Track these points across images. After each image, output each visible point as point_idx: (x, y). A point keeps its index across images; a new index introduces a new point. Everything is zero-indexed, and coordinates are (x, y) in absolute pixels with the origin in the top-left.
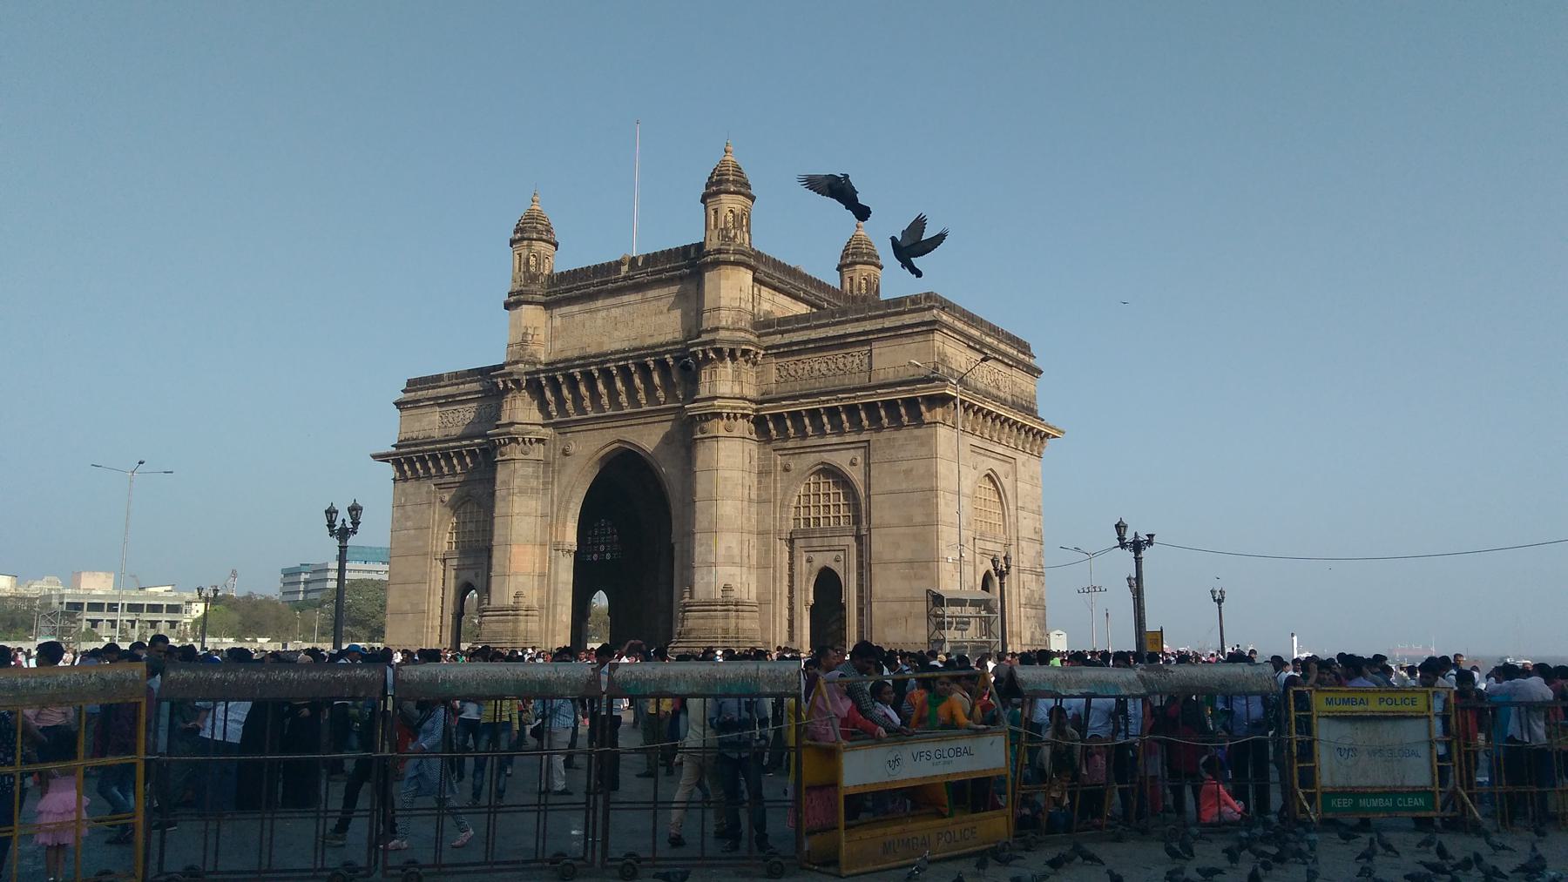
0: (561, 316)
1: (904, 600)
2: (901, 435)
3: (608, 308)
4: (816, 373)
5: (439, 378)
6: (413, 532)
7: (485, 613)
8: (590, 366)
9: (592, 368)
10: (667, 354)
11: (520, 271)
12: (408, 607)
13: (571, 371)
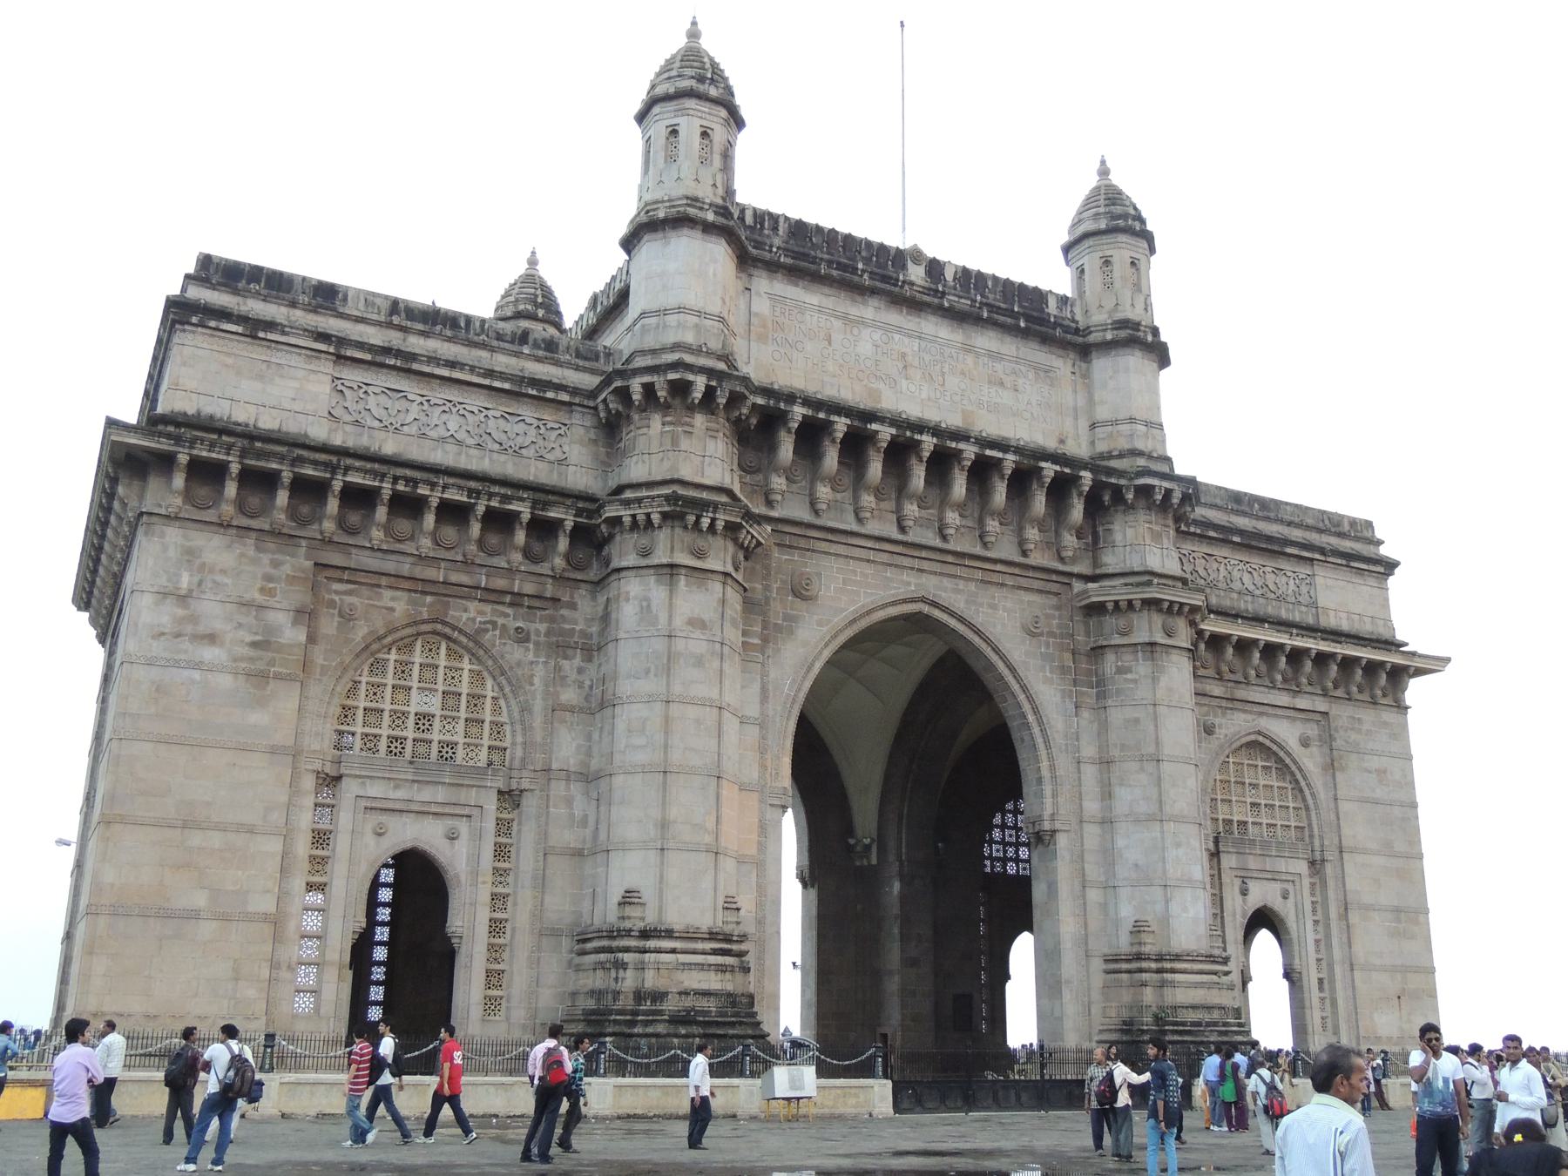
0: (773, 297)
1: (1394, 969)
2: (1367, 716)
3: (886, 328)
4: (1237, 585)
5: (326, 295)
6: (225, 681)
7: (652, 944)
8: (921, 433)
9: (925, 438)
10: (1085, 468)
11: (704, 161)
12: (200, 900)
13: (874, 427)
